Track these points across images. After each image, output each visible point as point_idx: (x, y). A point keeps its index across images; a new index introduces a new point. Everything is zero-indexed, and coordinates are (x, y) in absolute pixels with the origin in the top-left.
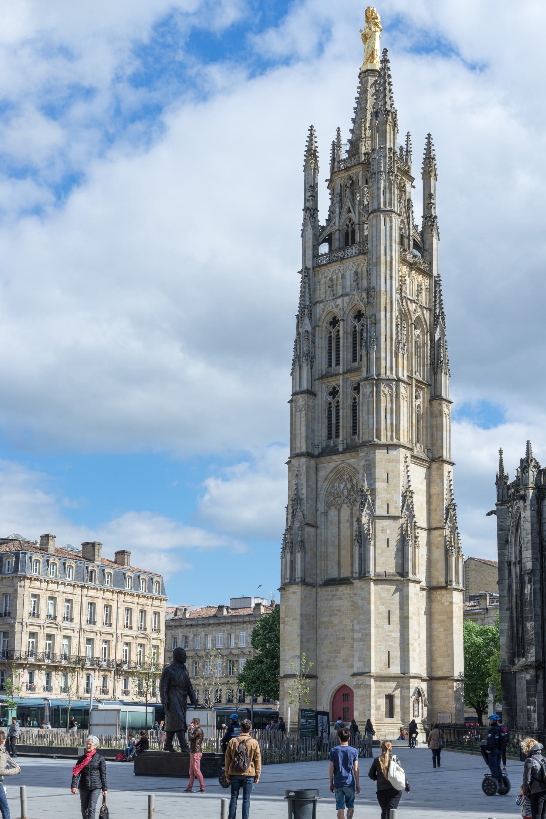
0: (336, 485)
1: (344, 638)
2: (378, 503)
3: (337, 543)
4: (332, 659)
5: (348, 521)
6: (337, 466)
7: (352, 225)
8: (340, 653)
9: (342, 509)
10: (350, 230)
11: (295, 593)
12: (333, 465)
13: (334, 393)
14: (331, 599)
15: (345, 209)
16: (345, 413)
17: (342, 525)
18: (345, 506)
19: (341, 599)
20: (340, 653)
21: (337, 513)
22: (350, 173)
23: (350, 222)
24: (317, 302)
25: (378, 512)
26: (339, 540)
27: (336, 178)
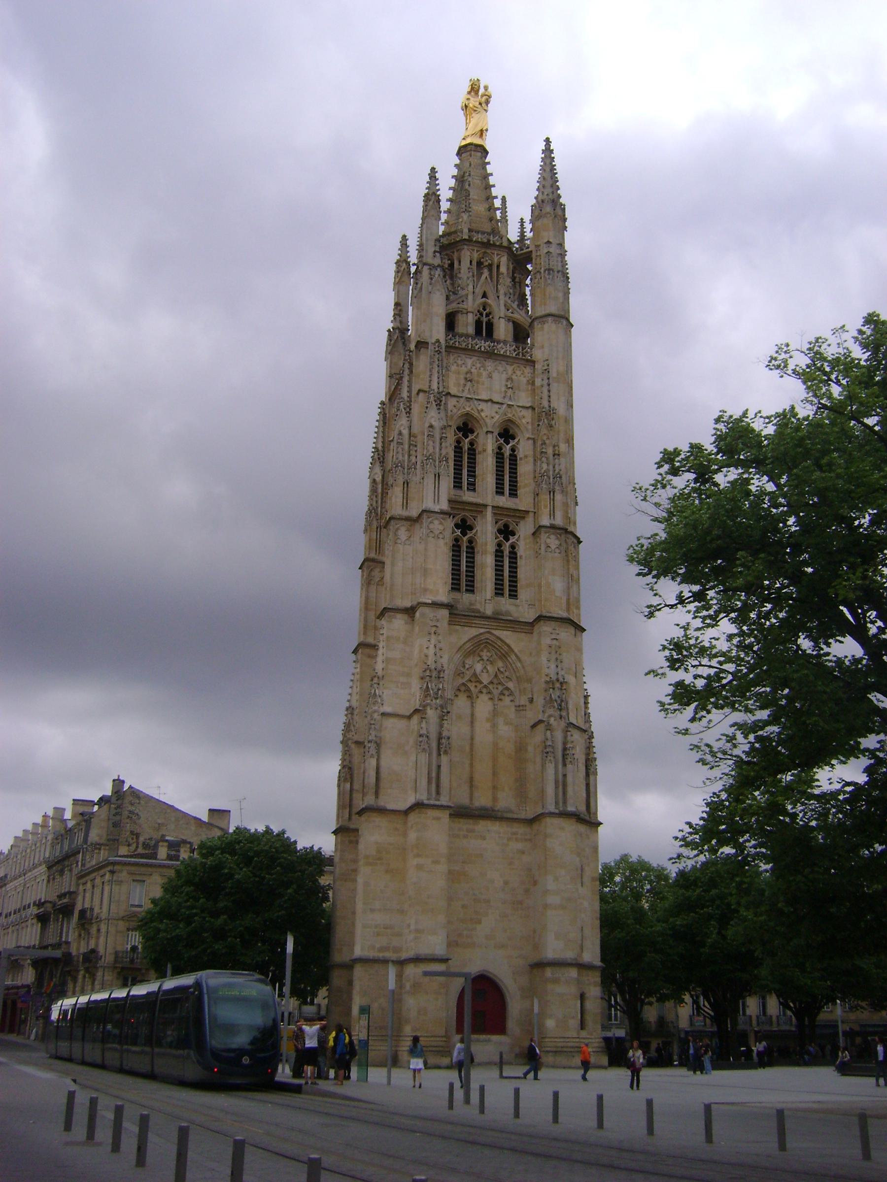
0: (469, 662)
1: (488, 901)
2: (570, 706)
3: (467, 749)
4: (465, 932)
5: (488, 720)
6: (481, 634)
7: (487, 315)
8: (480, 922)
9: (479, 701)
10: (485, 319)
11: (438, 819)
12: (474, 632)
13: (464, 526)
14: (465, 837)
15: (479, 291)
16: (486, 562)
17: (477, 724)
18: (484, 697)
19: (484, 838)
20: (480, 922)
21: (469, 703)
22: (488, 251)
24: (448, 394)
25: (573, 720)
26: (472, 745)
27: (466, 247)
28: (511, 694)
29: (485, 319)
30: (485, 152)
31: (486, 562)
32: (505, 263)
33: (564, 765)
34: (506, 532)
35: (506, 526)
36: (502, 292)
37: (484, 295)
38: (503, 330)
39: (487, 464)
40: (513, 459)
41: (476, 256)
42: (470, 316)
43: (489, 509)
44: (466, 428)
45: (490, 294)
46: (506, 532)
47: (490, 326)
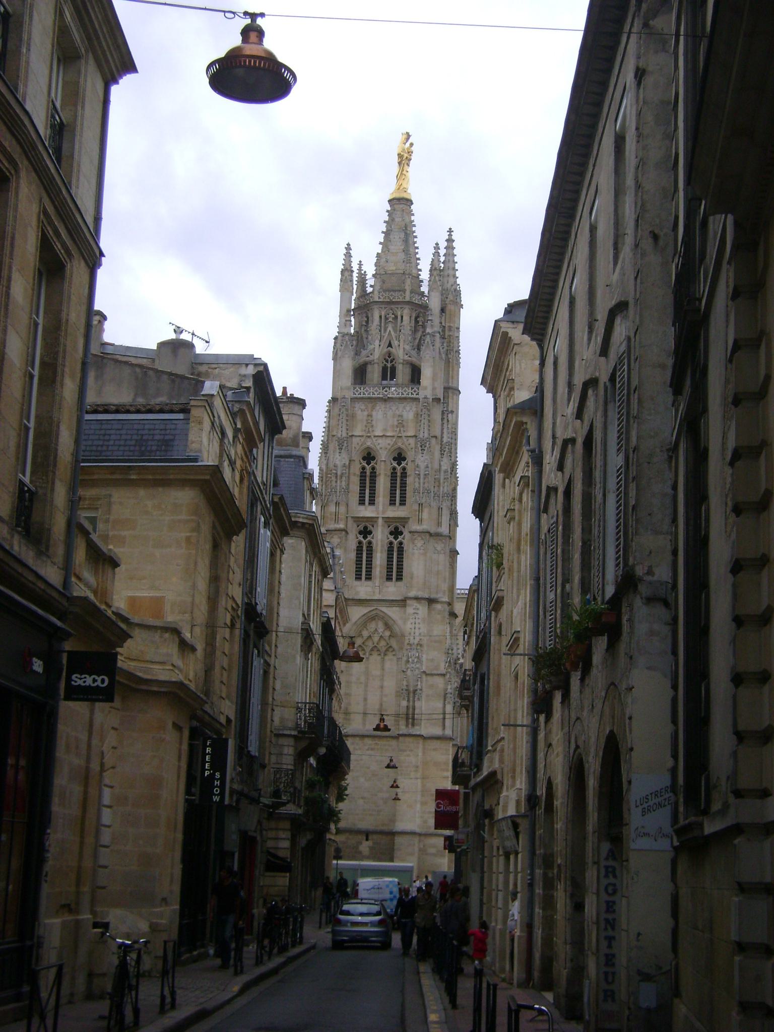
10: (389, 365)
13: (366, 532)
16: (379, 559)
23: (389, 357)
28: (394, 650)
29: (389, 365)
30: (409, 202)
31: (379, 559)
32: (406, 313)
33: (414, 701)
34: (396, 533)
35: (396, 528)
36: (402, 341)
37: (390, 345)
38: (402, 373)
39: (383, 484)
40: (404, 474)
41: (383, 314)
42: (376, 366)
43: (380, 521)
44: (369, 457)
45: (395, 343)
46: (396, 533)
47: (393, 369)
